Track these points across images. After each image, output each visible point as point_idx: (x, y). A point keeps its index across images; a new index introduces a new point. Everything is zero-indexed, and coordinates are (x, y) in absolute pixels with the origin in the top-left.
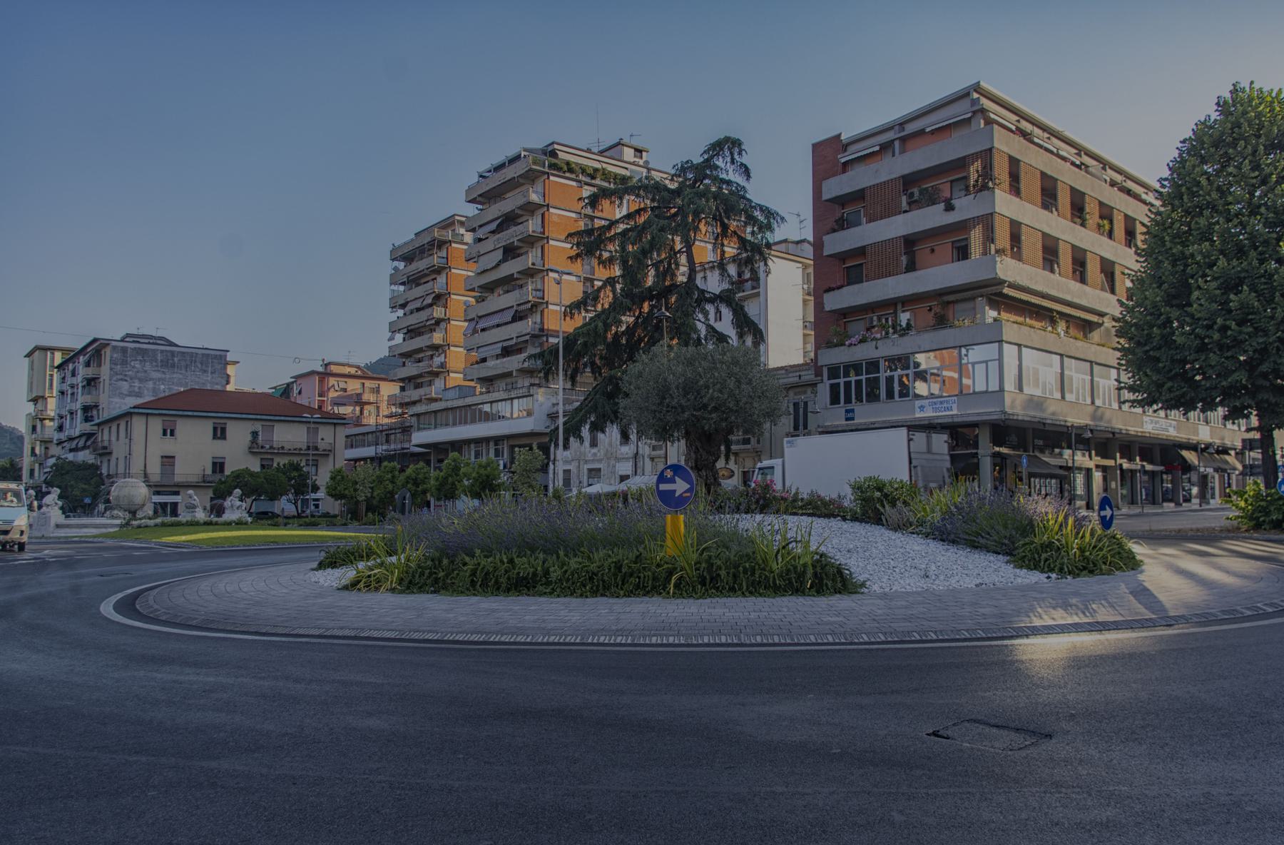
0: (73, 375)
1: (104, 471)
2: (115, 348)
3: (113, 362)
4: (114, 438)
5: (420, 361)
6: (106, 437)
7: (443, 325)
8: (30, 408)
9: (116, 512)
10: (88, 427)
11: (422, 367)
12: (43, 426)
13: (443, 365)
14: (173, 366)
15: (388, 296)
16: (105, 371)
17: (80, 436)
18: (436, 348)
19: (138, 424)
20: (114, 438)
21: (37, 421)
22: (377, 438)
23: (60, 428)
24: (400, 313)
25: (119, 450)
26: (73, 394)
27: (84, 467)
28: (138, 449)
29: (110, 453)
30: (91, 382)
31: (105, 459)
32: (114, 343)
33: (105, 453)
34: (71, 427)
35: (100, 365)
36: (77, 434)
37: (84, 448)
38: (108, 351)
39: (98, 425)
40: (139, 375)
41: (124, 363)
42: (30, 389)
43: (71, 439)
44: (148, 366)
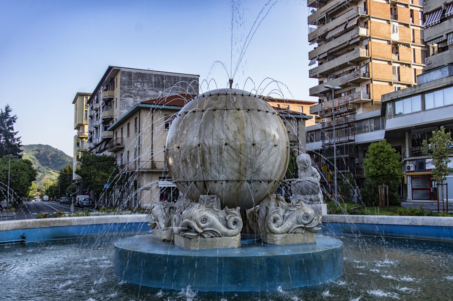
0: (97, 102)
1: (119, 163)
2: (123, 73)
3: (122, 83)
4: (125, 136)
5: (337, 77)
6: (119, 136)
7: (365, 42)
8: (76, 132)
9: (198, 211)
10: (107, 134)
11: (347, 78)
12: (83, 142)
13: (368, 73)
14: (163, 86)
15: (307, 33)
16: (117, 93)
17: (102, 142)
18: (359, 61)
19: (145, 119)
20: (125, 136)
21: (79, 140)
22: (323, 134)
23: (91, 140)
24: (316, 45)
25: (130, 144)
26: (97, 116)
27: (105, 159)
28: (146, 138)
29: (123, 148)
30: (109, 102)
31: (119, 154)
32: (123, 70)
33: (120, 149)
34: (97, 137)
35: (113, 89)
36: (100, 140)
37: (105, 149)
38: (119, 76)
39: (113, 129)
40: (140, 93)
41: (130, 84)
42: (76, 122)
43: (97, 146)
44: (146, 87)
